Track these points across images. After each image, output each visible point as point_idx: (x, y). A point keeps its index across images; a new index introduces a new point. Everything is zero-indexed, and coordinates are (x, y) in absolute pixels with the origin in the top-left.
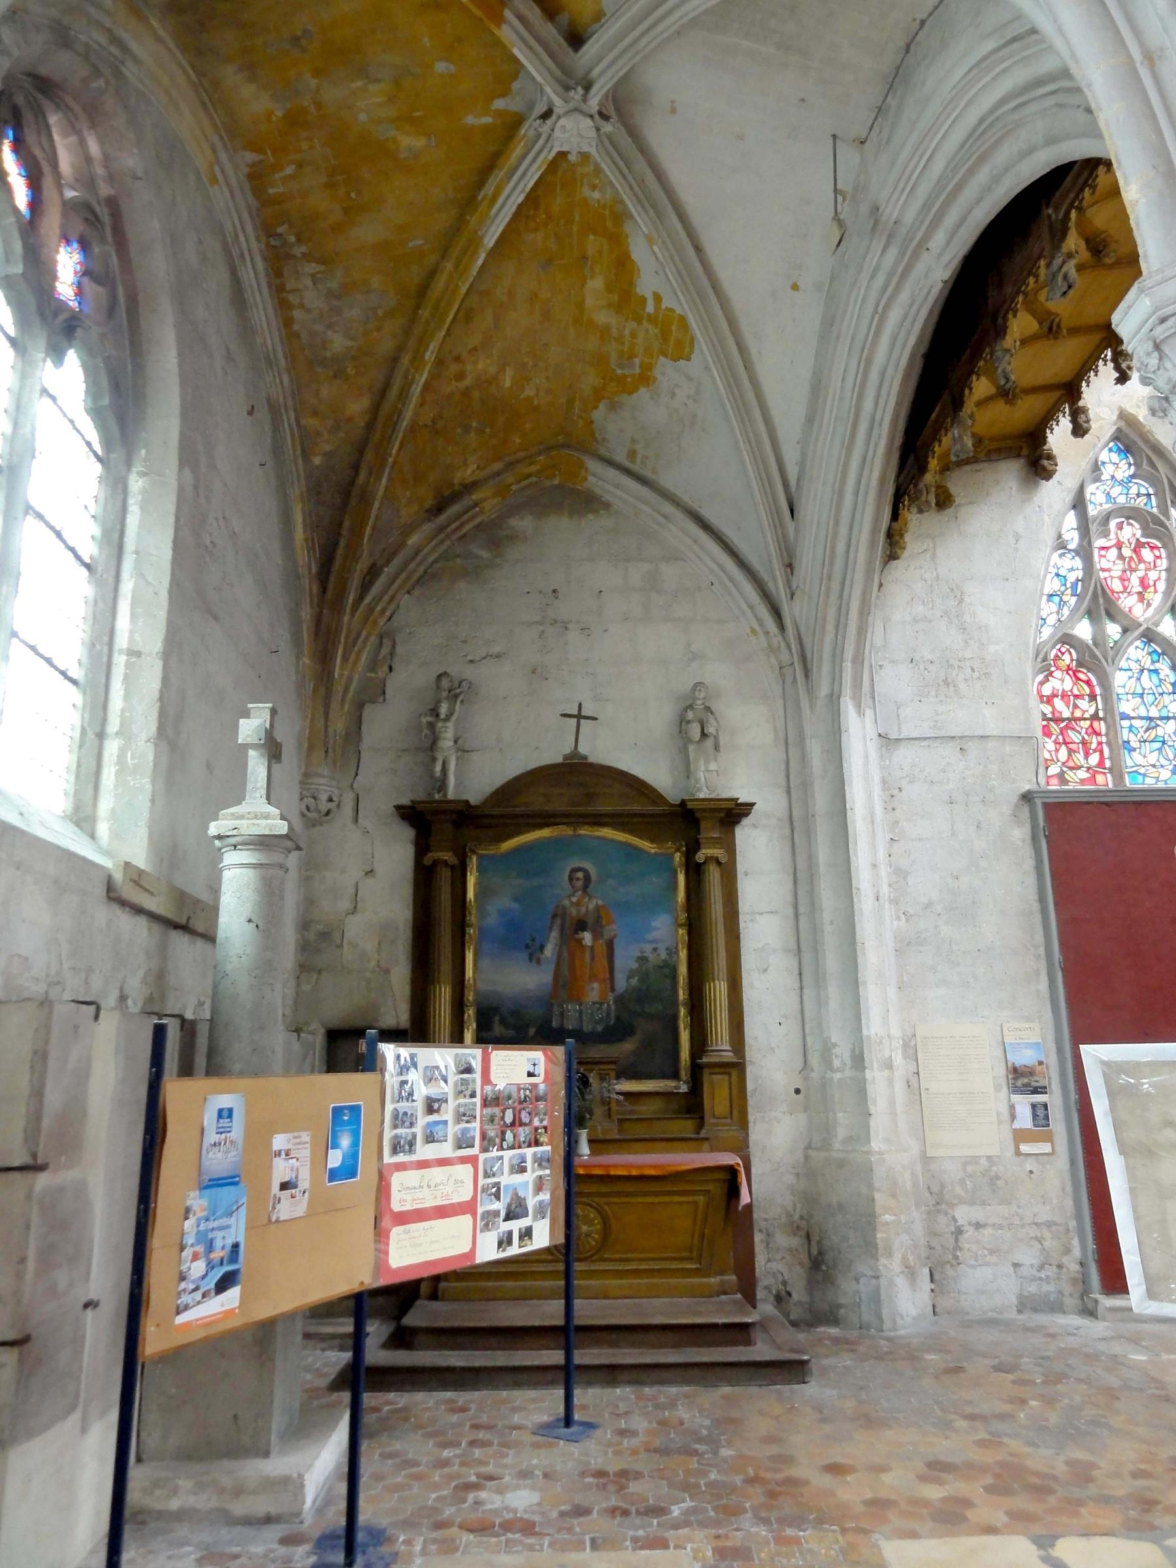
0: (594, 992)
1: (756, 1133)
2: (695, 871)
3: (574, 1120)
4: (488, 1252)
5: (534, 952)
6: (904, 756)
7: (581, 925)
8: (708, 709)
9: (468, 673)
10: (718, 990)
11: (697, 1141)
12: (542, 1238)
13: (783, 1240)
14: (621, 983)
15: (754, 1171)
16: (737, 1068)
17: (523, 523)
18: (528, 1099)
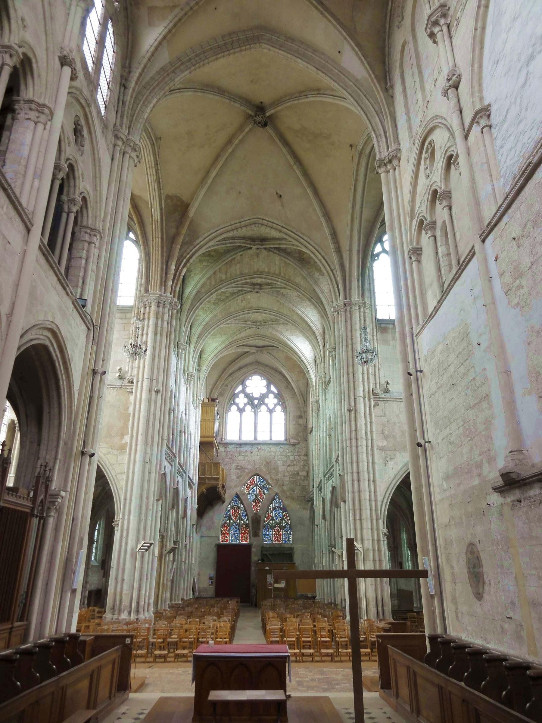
6: (203, 538)
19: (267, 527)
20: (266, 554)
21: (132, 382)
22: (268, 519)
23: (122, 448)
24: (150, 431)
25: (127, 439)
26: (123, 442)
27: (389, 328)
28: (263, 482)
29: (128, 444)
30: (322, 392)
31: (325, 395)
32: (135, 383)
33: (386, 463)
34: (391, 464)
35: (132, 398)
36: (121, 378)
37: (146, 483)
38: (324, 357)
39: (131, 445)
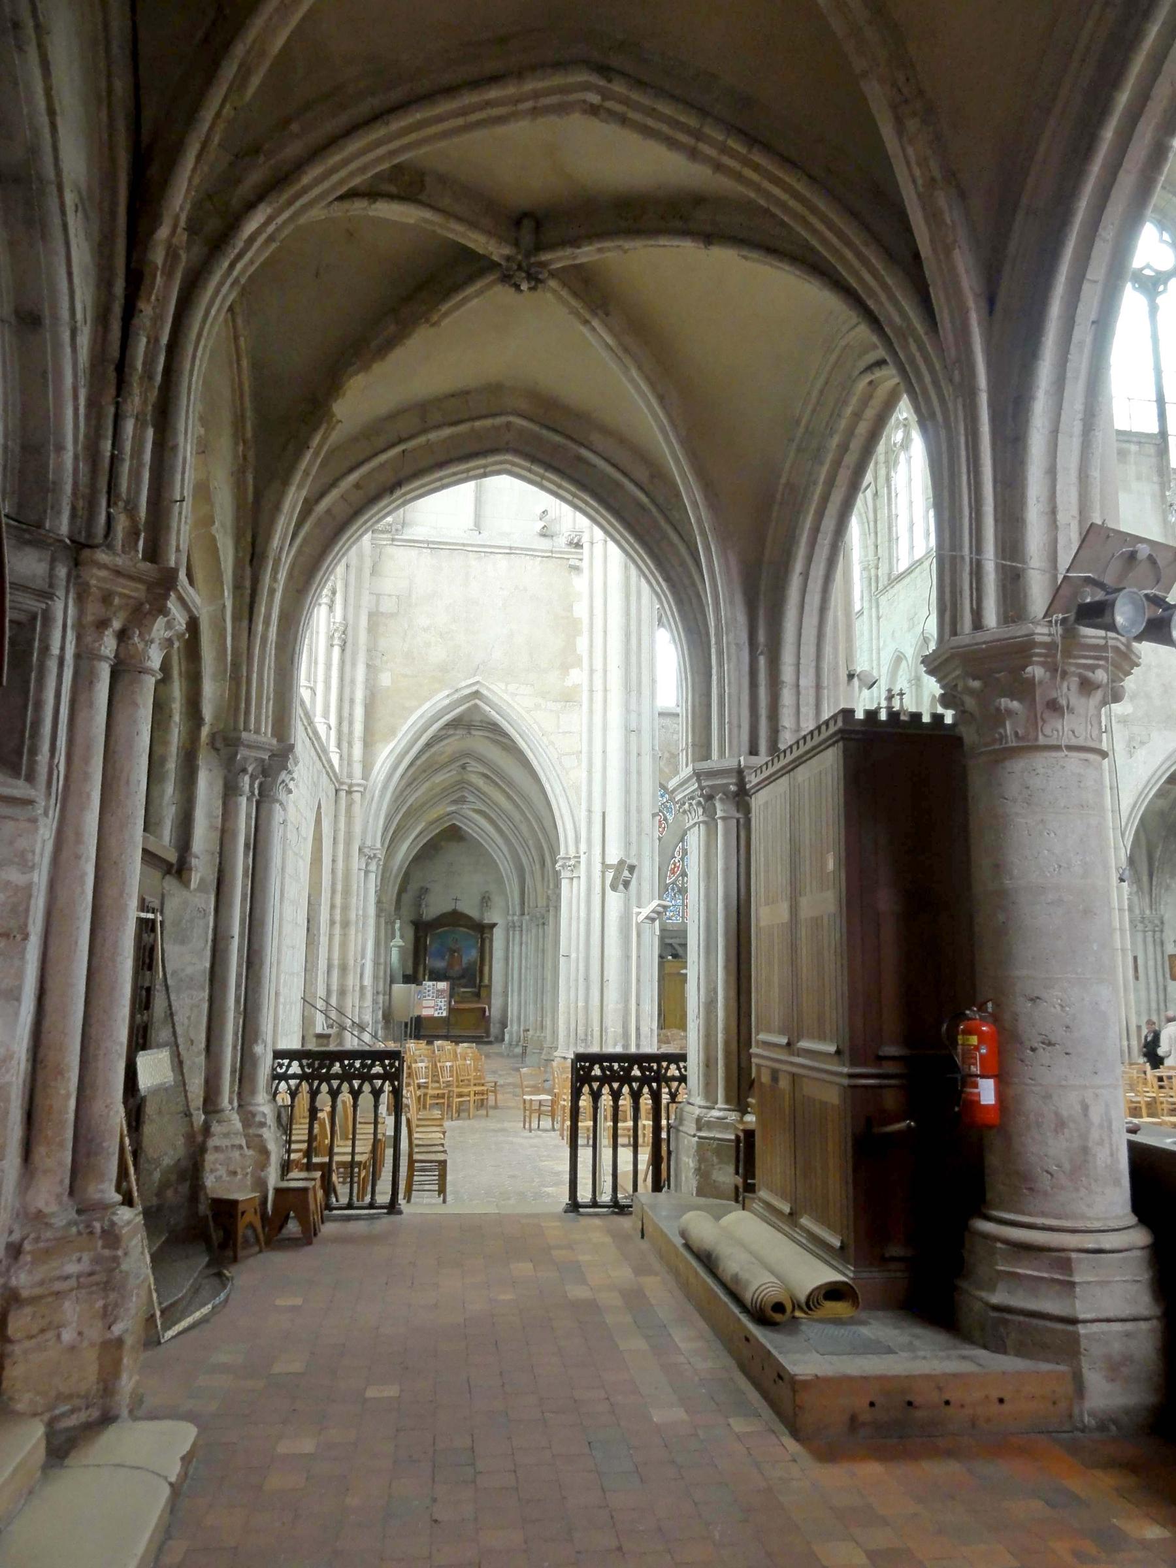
0: (457, 968)
1: (493, 1001)
2: (483, 940)
3: (451, 996)
4: (436, 1015)
5: (443, 958)
7: (455, 951)
8: (489, 898)
9: (428, 886)
10: (486, 969)
11: (478, 1002)
12: (445, 1014)
13: (498, 1025)
14: (464, 965)
15: (492, 1010)
16: (489, 987)
17: (443, 843)
18: (442, 991)
19: (673, 889)
20: (671, 945)
21: (578, 545)
22: (673, 873)
23: (568, 698)
24: (634, 659)
25: (577, 676)
26: (569, 682)
27: (1129, 452)
28: (662, 796)
29: (585, 688)
30: (870, 601)
31: (878, 607)
32: (586, 546)
33: (1131, 750)
34: (1141, 753)
35: (580, 583)
36: (545, 534)
37: (634, 776)
38: (876, 521)
39: (591, 691)
